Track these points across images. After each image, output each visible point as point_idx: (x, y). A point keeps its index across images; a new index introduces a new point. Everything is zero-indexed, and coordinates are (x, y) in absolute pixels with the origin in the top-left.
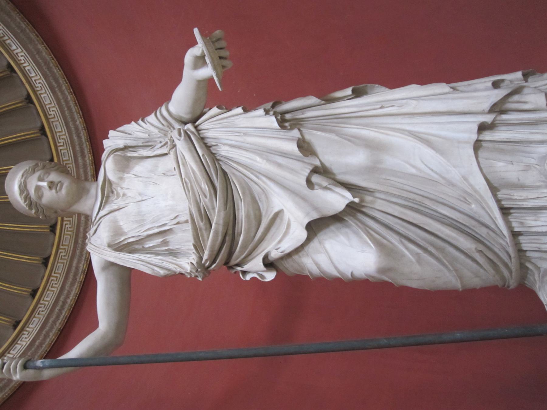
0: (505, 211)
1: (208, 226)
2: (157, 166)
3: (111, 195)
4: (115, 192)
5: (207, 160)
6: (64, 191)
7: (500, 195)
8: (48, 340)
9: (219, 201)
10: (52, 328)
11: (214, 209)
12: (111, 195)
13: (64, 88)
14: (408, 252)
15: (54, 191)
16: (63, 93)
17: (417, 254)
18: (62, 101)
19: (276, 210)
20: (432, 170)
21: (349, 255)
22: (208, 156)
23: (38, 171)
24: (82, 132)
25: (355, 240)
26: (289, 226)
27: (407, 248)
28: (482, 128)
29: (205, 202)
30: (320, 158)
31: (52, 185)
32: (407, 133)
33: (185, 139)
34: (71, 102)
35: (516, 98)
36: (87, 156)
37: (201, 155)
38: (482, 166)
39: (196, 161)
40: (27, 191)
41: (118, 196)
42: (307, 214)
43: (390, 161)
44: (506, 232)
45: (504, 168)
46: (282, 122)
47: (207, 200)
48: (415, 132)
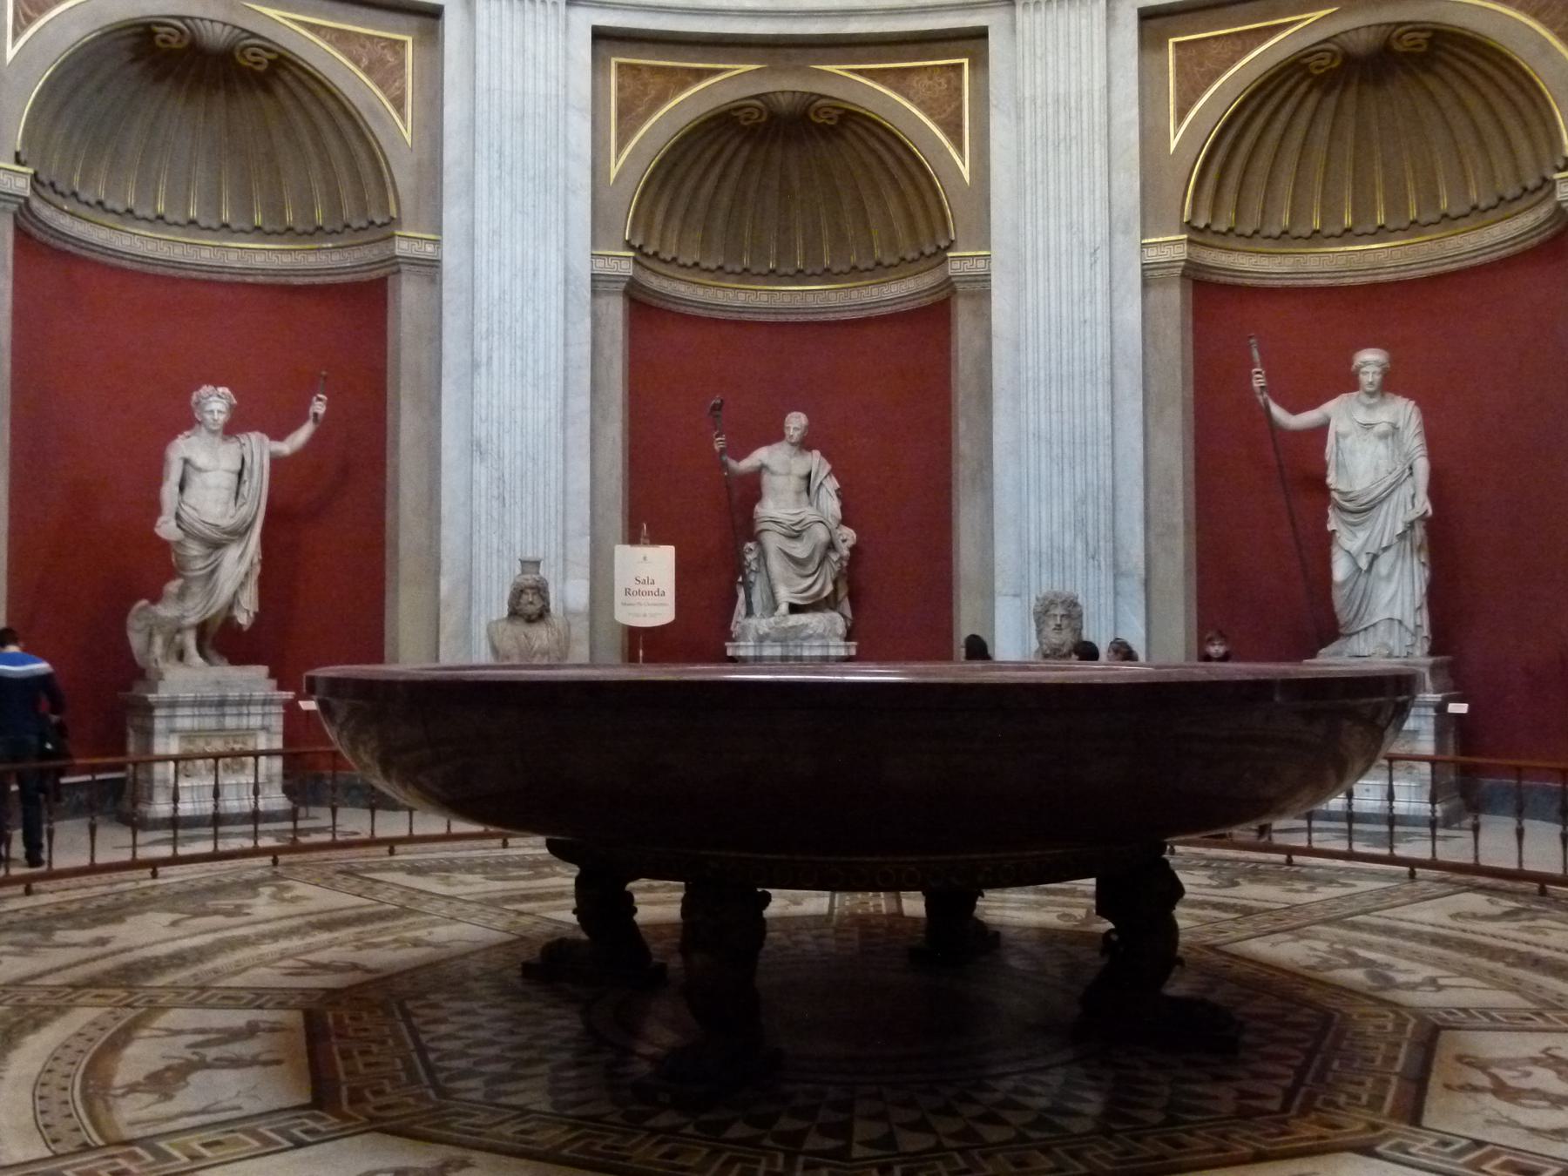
14: (1346, 591)
21: (1340, 569)
28: (1400, 622)
45: (1381, 628)
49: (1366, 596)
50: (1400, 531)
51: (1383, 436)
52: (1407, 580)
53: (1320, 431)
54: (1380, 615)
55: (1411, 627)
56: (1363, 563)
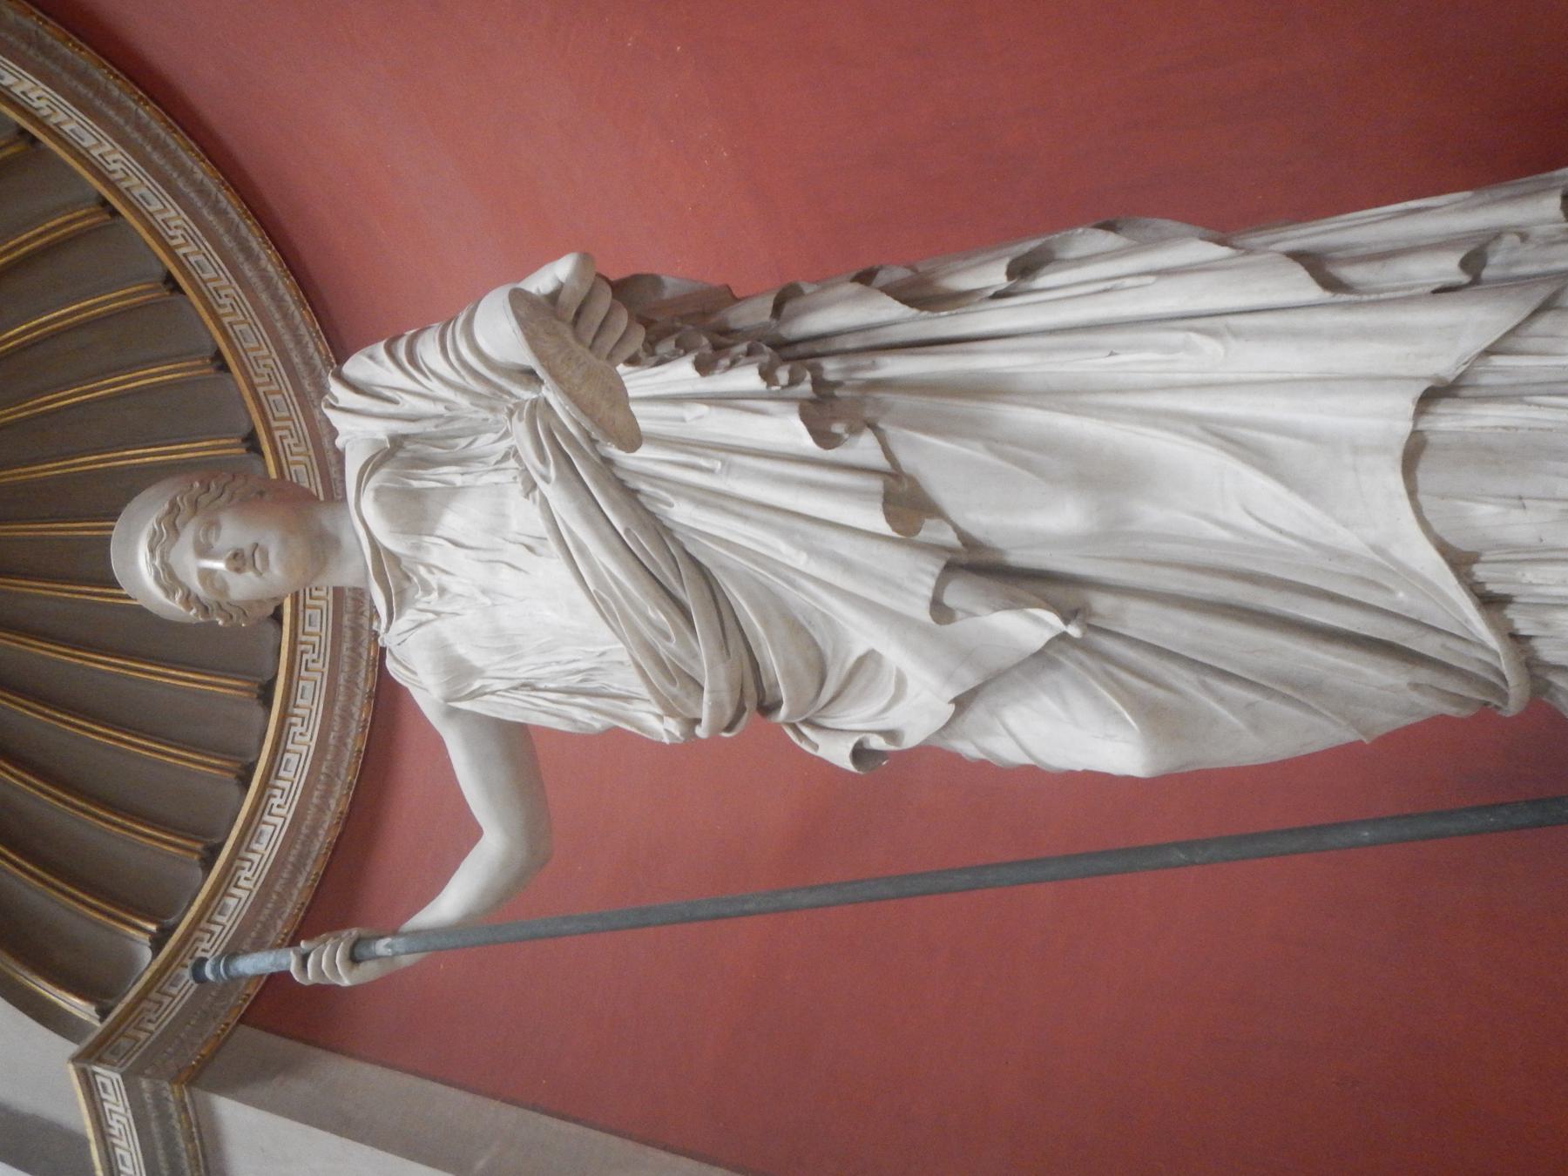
0: (1491, 602)
1: (691, 687)
2: (503, 515)
3: (406, 585)
4: (415, 579)
5: (645, 545)
6: (276, 571)
7: (1480, 572)
8: (354, 725)
9: (706, 645)
10: (350, 697)
11: (695, 656)
12: (406, 585)
13: (116, 93)
15: (250, 574)
16: (119, 107)
17: (1250, 705)
18: (128, 129)
19: (859, 650)
20: (1281, 532)
22: (641, 533)
23: (184, 524)
24: (221, 197)
25: (1080, 704)
26: (901, 682)
27: (1221, 700)
29: (668, 649)
30: (954, 515)
31: (238, 560)
32: (1193, 429)
33: (560, 478)
34: (154, 125)
35: (1545, 323)
36: (263, 256)
37: (621, 532)
38: (1429, 517)
39: (613, 553)
40: (181, 584)
41: (427, 589)
42: (949, 677)
43: (1151, 515)
44: (1493, 642)
46: (825, 413)
47: (673, 645)
48: (1220, 420)
49: (1250, 598)
50: (787, 429)
51: (415, 512)
52: (1137, 361)
53: (518, 746)
54: (1374, 529)
55: (1479, 321)
56: (1029, 627)
